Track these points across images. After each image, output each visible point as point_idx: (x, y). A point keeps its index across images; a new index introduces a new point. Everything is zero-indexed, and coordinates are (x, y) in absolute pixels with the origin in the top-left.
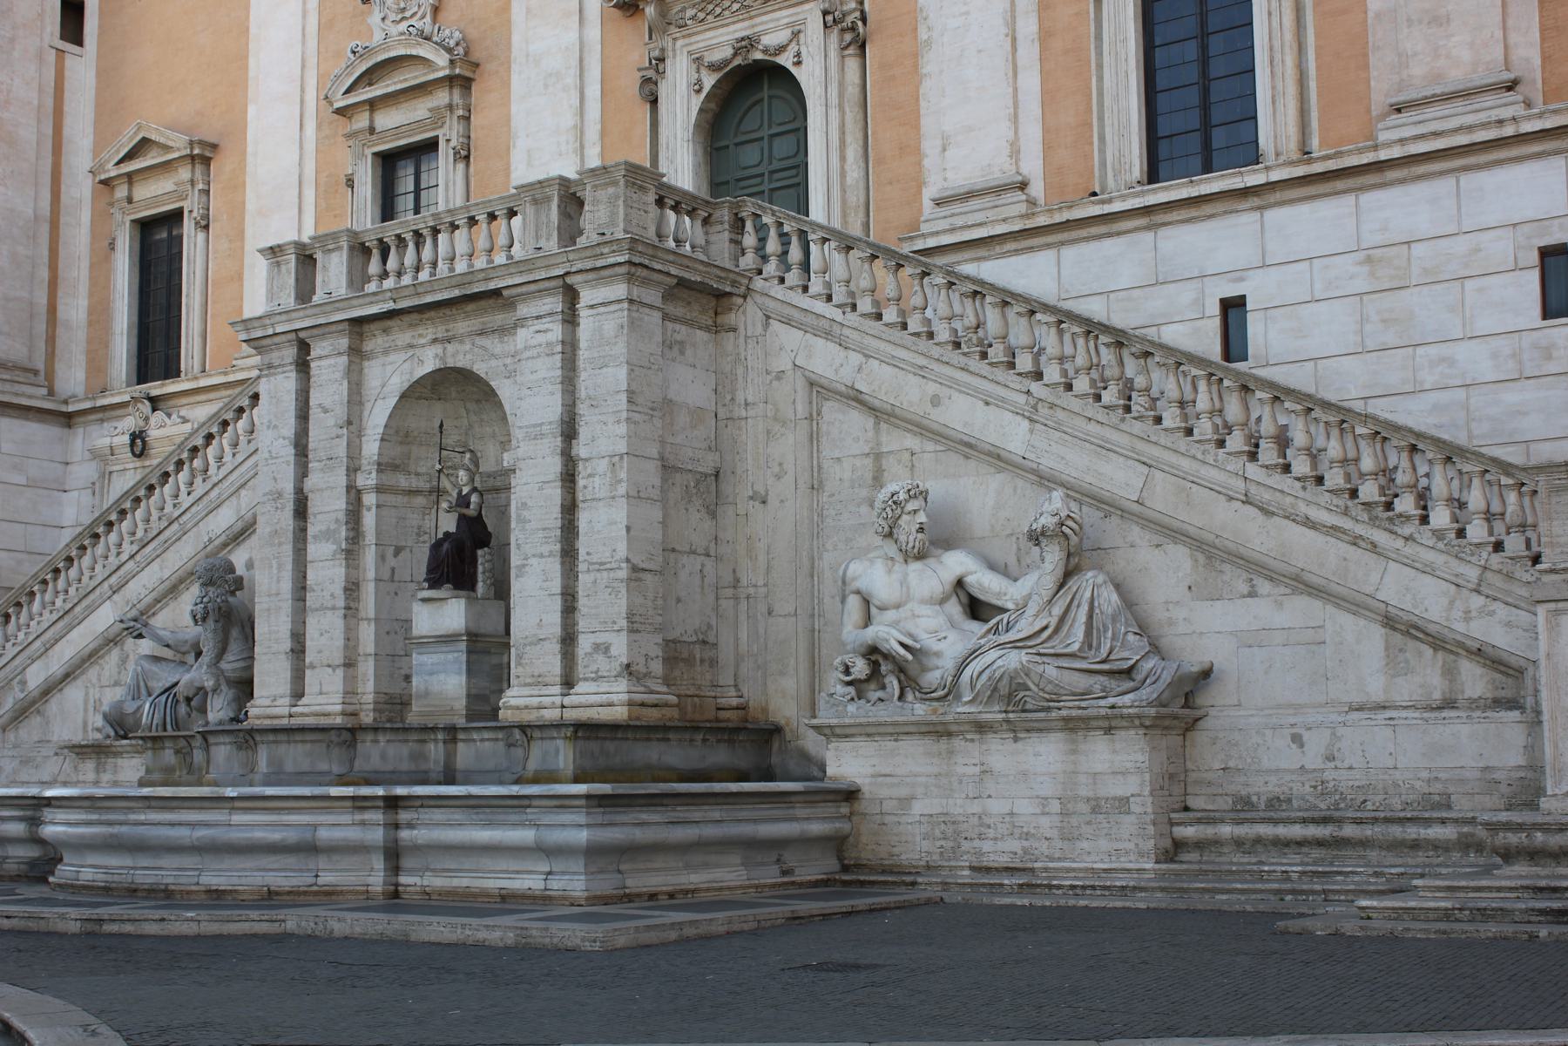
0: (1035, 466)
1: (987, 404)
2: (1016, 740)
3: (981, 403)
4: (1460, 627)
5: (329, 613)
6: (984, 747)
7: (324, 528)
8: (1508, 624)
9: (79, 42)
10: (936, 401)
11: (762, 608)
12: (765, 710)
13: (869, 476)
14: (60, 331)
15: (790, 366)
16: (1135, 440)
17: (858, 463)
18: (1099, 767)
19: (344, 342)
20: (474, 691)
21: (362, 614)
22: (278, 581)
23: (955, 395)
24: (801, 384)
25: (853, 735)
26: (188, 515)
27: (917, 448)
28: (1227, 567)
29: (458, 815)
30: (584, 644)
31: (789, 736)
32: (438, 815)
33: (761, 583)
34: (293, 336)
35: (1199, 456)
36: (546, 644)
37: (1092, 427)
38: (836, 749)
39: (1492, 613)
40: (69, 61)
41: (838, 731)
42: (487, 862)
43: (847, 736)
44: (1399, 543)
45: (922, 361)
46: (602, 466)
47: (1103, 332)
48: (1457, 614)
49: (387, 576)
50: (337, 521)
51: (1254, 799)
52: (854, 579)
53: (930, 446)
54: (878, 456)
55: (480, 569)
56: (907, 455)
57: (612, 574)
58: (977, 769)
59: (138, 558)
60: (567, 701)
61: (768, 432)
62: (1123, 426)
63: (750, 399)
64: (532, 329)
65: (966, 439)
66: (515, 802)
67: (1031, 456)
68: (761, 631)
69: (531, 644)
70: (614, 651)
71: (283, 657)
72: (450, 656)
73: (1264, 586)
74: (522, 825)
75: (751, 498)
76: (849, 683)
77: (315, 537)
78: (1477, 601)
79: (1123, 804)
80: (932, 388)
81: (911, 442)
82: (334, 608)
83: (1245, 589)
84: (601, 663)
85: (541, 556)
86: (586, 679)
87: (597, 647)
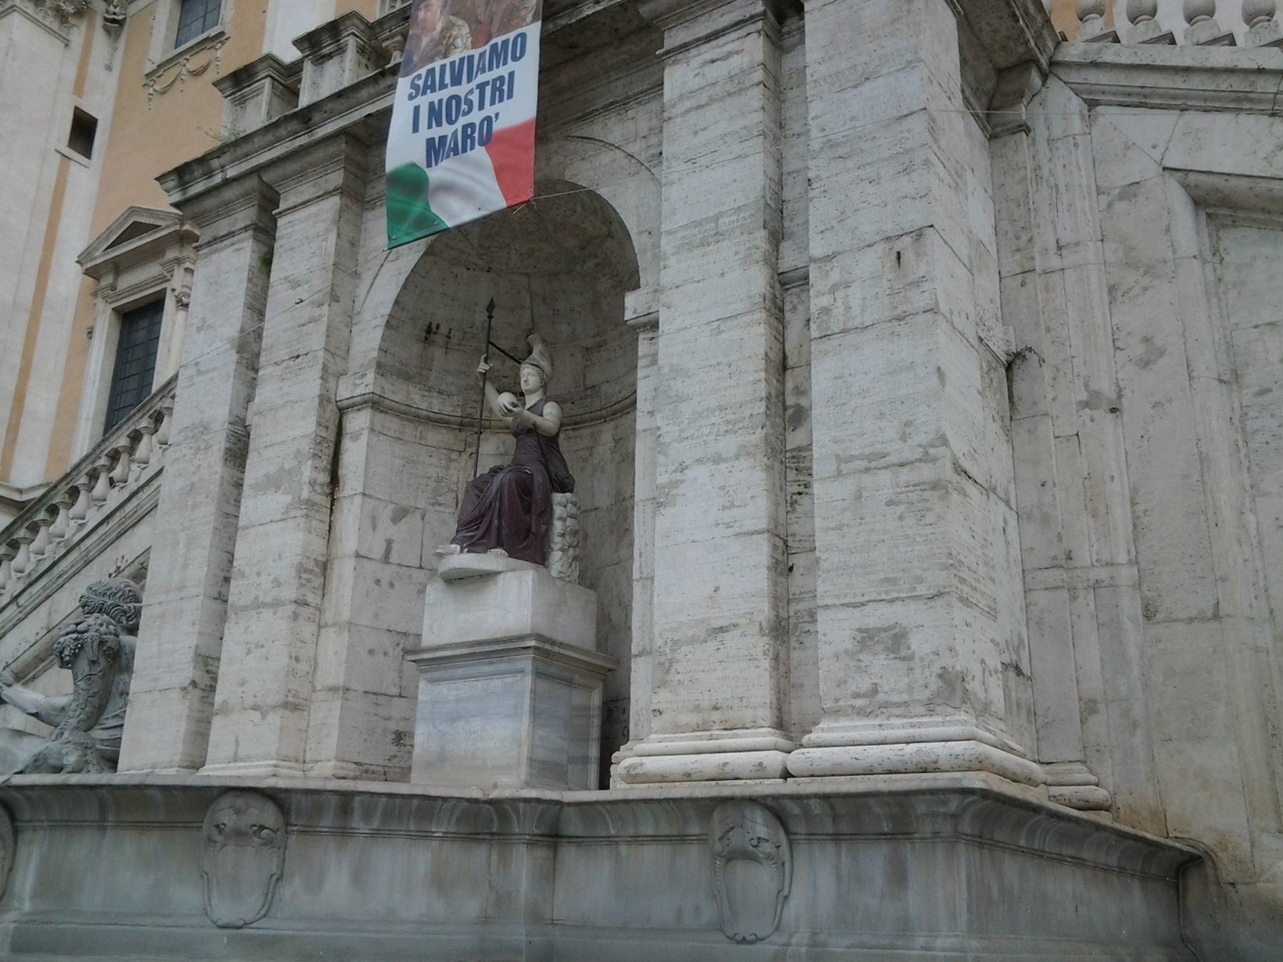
5: (267, 614)
7: (273, 469)
9: (87, 153)
11: (1130, 607)
12: (1159, 816)
14: (25, 421)
15: (1154, 170)
19: (336, 178)
20: (540, 754)
21: (329, 617)
22: (185, 566)
24: (1179, 201)
26: (94, 538)
30: (834, 631)
31: (1229, 872)
33: (1122, 558)
34: (252, 183)
36: (731, 638)
40: (73, 168)
46: (872, 261)
49: (378, 552)
50: (298, 452)
55: (558, 526)
57: (905, 475)
59: (21, 601)
60: (796, 760)
61: (1112, 289)
63: (1066, 238)
64: (695, 63)
68: (1133, 651)
69: (693, 641)
70: (919, 643)
71: (176, 695)
72: (496, 683)
75: (1086, 404)
77: (251, 486)
82: (276, 604)
84: (882, 670)
85: (718, 460)
86: (836, 713)
87: (866, 638)
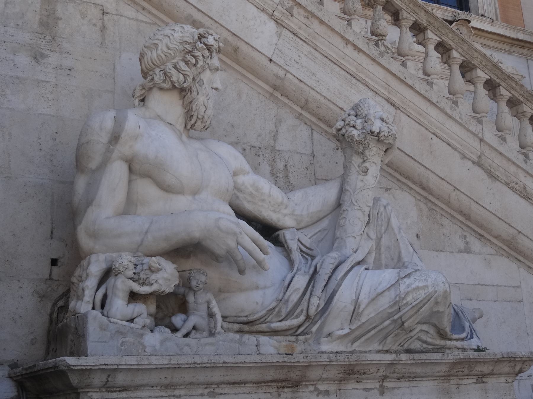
0: (281, 73)
28: (446, 221)
37: (349, 50)
41: (120, 379)
67: (281, 62)
73: (476, 245)
83: (461, 244)
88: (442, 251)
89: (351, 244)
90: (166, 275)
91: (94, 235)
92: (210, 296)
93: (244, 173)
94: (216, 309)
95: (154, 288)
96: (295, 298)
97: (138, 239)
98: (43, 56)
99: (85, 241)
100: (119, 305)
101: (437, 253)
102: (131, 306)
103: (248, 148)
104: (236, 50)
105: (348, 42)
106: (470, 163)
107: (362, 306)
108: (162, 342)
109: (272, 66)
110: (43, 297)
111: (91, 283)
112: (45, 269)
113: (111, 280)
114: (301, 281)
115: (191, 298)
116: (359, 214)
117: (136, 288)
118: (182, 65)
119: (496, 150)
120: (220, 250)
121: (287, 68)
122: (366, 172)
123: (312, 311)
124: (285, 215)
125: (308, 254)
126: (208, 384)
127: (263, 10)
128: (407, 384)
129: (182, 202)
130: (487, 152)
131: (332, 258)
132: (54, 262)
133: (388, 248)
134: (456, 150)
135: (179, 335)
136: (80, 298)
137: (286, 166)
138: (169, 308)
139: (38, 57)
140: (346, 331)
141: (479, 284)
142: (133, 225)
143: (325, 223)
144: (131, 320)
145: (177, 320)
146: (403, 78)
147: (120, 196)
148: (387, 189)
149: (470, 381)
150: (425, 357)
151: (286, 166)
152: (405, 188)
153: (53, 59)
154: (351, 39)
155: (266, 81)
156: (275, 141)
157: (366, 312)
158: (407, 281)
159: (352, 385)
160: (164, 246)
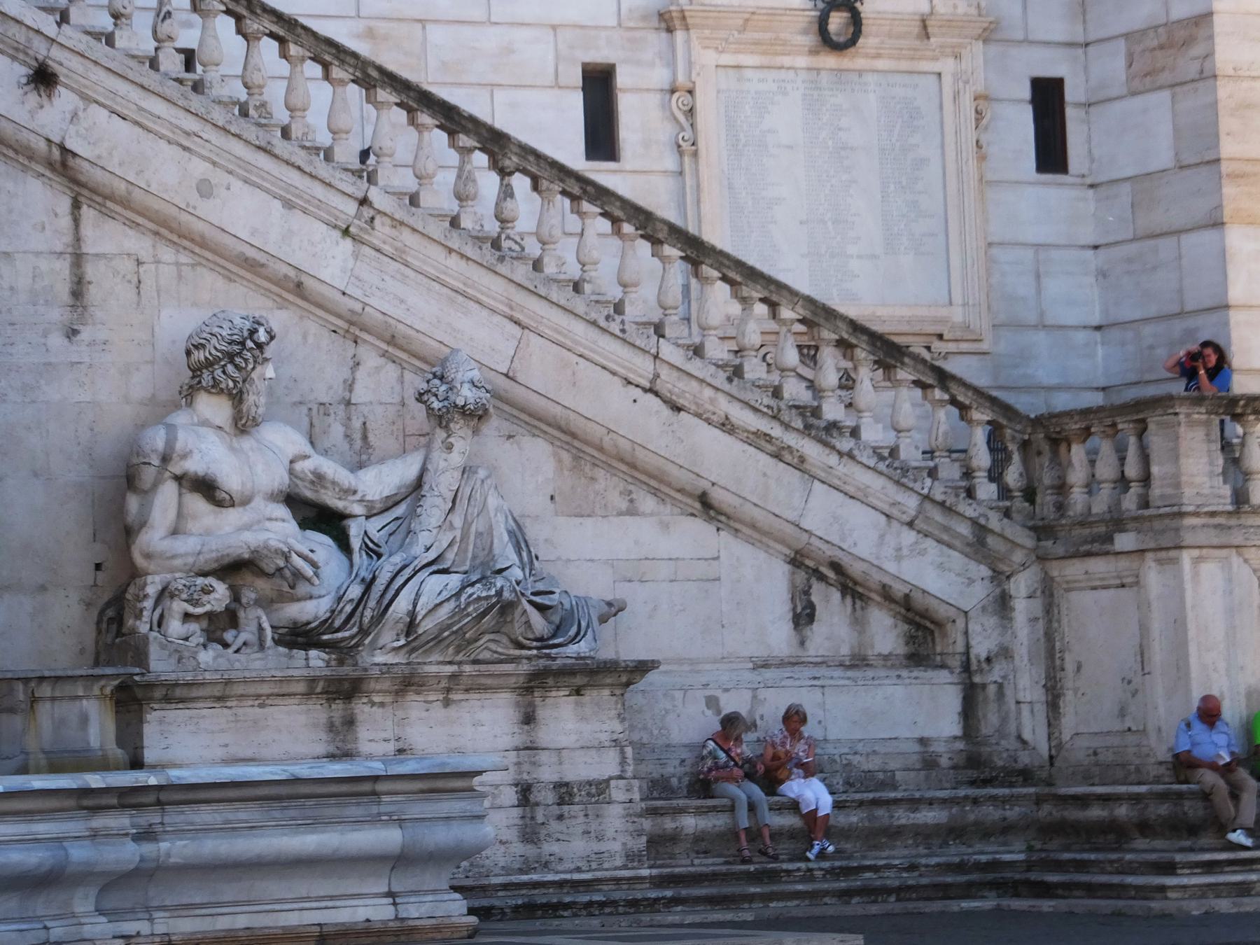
0: (357, 307)
1: (288, 205)
2: (447, 703)
3: (277, 204)
4: (891, 567)
6: (400, 714)
8: (941, 566)
10: (205, 189)
13: (63, 290)
16: (512, 289)
17: (44, 265)
18: (563, 741)
23: (237, 184)
25: (193, 699)
27: (144, 255)
28: (600, 473)
29: (245, 814)
32: (206, 815)
35: (603, 323)
37: (453, 262)
38: (161, 722)
39: (923, 553)
41: (178, 692)
42: (273, 887)
43: (182, 700)
44: (833, 459)
45: (191, 124)
47: (467, 132)
48: (888, 551)
51: (674, 781)
52: (184, 456)
53: (167, 254)
54: (78, 259)
56: (130, 265)
58: (391, 747)
62: (501, 268)
65: (251, 253)
66: (344, 788)
67: (357, 293)
73: (648, 503)
74: (375, 820)
76: (187, 617)
78: (909, 537)
79: (599, 789)
80: (199, 168)
81: (138, 243)
83: (624, 505)
88: (589, 516)
89: (424, 539)
90: (217, 596)
91: (148, 556)
92: (260, 612)
93: (306, 457)
94: (266, 625)
95: (208, 608)
96: (349, 608)
97: (190, 560)
98: (75, 332)
99: (139, 560)
100: (175, 627)
101: (581, 520)
102: (186, 626)
103: (315, 407)
104: (299, 285)
105: (450, 250)
106: (638, 393)
107: (419, 618)
108: (215, 658)
109: (346, 299)
110: (89, 605)
111: (148, 604)
112: (88, 575)
113: (167, 602)
114: (355, 591)
115: (241, 614)
116: (439, 501)
117: (191, 609)
118: (230, 368)
119: (680, 370)
120: (270, 568)
121: (366, 300)
122: (450, 448)
123: (366, 620)
124: (353, 502)
125: (373, 552)
126: (258, 696)
127: (335, 227)
128: (477, 696)
129: (232, 517)
130: (665, 372)
131: (398, 559)
132: (98, 567)
133: (479, 535)
134: (614, 373)
135: (230, 651)
136: (139, 616)
137: (364, 423)
138: (219, 626)
139: (72, 333)
140: (402, 642)
141: (647, 559)
142: (186, 545)
143: (400, 510)
144: (186, 639)
145: (229, 636)
146: (532, 288)
147: (172, 514)
148: (510, 437)
149: (562, 693)
150: (492, 668)
151: (364, 423)
152: (537, 432)
153: (86, 334)
154: (455, 247)
155: (339, 316)
156: (351, 391)
157: (423, 624)
158: (470, 590)
159: (411, 696)
160: (215, 565)
